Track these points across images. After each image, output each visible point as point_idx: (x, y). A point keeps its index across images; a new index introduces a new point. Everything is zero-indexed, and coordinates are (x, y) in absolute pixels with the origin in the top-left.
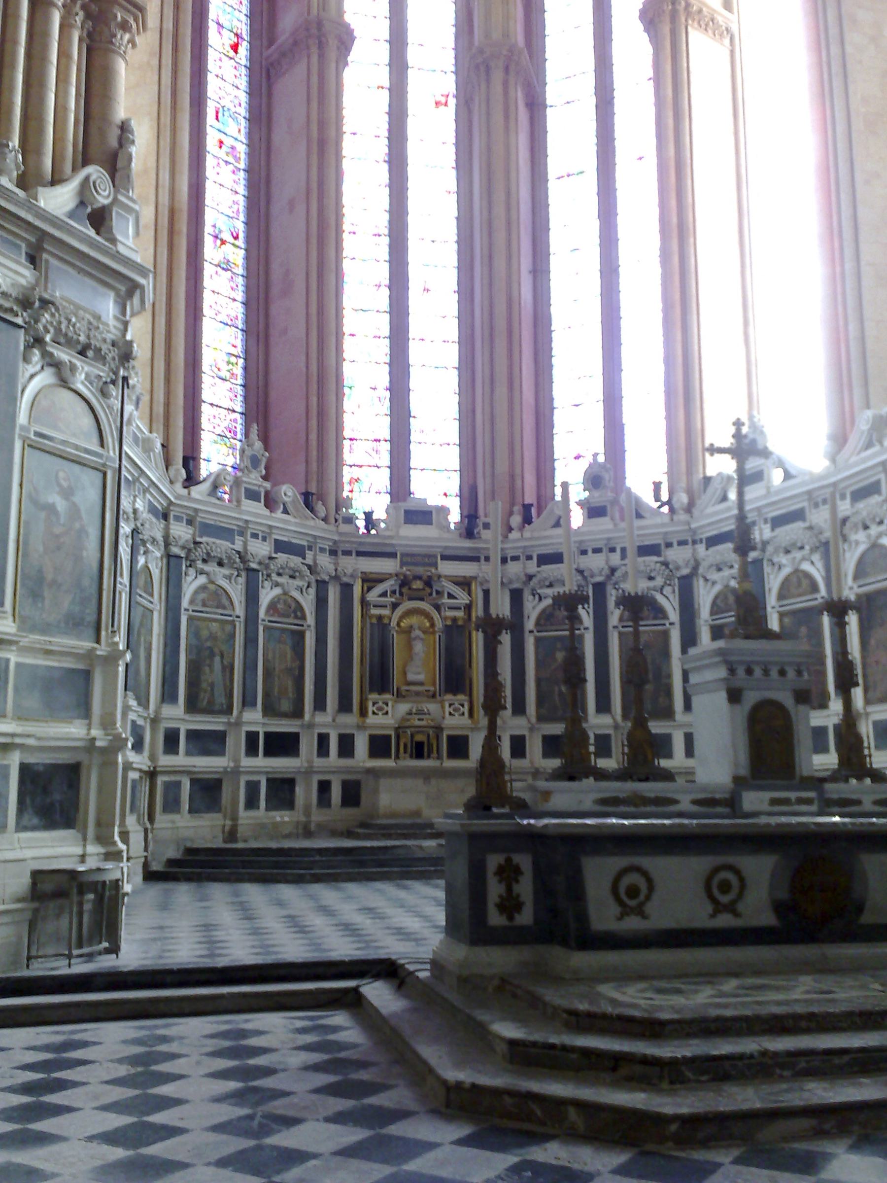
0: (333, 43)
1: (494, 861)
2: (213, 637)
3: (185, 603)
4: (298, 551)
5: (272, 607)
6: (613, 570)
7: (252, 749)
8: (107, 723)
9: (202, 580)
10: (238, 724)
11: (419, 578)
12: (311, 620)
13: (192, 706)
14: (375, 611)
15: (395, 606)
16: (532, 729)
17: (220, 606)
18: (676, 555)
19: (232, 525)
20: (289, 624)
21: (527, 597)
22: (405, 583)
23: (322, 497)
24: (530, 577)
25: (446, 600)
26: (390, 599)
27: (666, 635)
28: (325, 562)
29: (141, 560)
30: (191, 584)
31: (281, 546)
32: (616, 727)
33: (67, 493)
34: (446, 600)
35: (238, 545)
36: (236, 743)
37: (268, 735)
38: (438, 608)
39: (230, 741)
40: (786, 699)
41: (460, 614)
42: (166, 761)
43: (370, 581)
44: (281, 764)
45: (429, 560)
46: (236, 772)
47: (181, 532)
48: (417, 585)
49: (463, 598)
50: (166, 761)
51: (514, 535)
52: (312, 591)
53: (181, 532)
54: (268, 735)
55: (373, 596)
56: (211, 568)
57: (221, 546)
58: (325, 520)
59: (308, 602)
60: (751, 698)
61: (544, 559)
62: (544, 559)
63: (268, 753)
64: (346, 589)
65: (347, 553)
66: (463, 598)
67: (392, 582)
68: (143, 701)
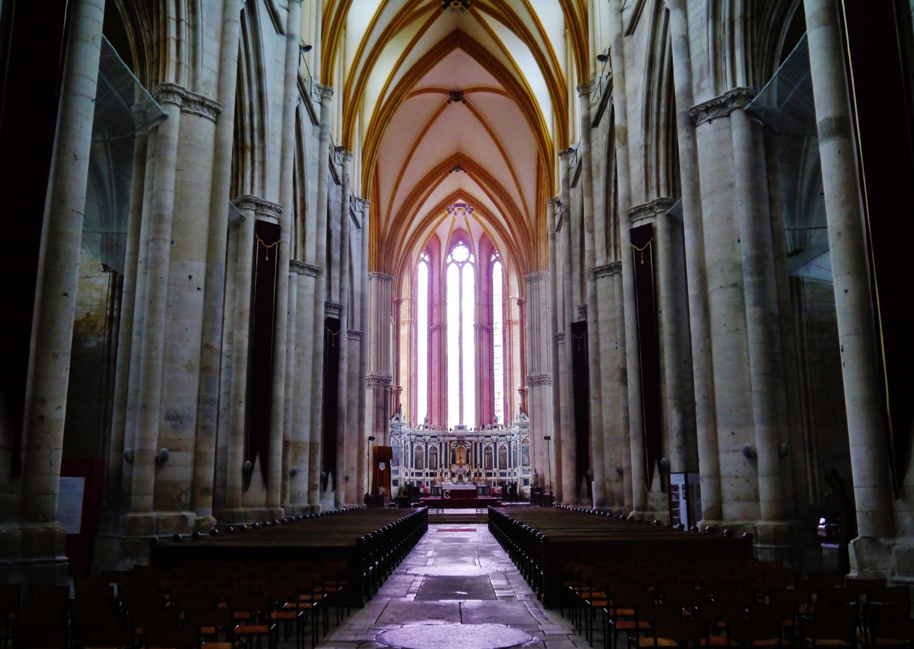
0: (443, 329)
1: (433, 489)
2: (419, 455)
3: (414, 450)
4: (435, 437)
5: (431, 448)
6: (497, 439)
7: (427, 475)
8: (401, 475)
9: (417, 445)
10: (424, 471)
11: (461, 440)
12: (439, 450)
13: (416, 468)
14: (452, 448)
15: (456, 446)
16: (483, 471)
17: (420, 449)
18: (508, 437)
19: (423, 434)
20: (434, 452)
21: (483, 445)
22: (458, 441)
23: (441, 425)
24: (483, 440)
25: (467, 445)
26: (455, 445)
27: (506, 453)
28: (442, 439)
29: (406, 444)
30: (415, 446)
31: (432, 437)
32: (497, 471)
33: (396, 451)
34: (467, 445)
35: (424, 437)
36: (424, 474)
37: (430, 473)
38: (465, 446)
39: (423, 474)
40: (462, 474)
41: (470, 448)
42: (412, 478)
43: (451, 442)
44: (432, 478)
45: (463, 437)
46: (424, 480)
47: (413, 437)
48: (461, 442)
49: (470, 445)
50: (412, 478)
51: (480, 431)
52: (439, 445)
53: (413, 437)
54: (430, 473)
55: (452, 445)
56: (419, 442)
57: (420, 438)
58: (442, 430)
59: (438, 447)
60: (459, 474)
61: (486, 437)
62: (486, 437)
63: (430, 476)
64: (446, 444)
65: (446, 436)
66: (470, 445)
67: (455, 442)
68: (407, 468)
